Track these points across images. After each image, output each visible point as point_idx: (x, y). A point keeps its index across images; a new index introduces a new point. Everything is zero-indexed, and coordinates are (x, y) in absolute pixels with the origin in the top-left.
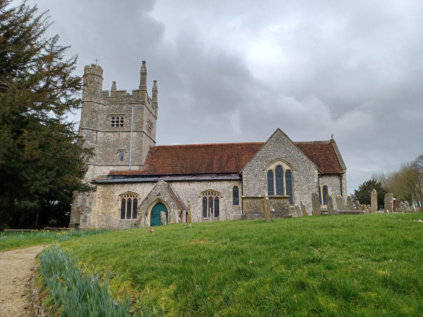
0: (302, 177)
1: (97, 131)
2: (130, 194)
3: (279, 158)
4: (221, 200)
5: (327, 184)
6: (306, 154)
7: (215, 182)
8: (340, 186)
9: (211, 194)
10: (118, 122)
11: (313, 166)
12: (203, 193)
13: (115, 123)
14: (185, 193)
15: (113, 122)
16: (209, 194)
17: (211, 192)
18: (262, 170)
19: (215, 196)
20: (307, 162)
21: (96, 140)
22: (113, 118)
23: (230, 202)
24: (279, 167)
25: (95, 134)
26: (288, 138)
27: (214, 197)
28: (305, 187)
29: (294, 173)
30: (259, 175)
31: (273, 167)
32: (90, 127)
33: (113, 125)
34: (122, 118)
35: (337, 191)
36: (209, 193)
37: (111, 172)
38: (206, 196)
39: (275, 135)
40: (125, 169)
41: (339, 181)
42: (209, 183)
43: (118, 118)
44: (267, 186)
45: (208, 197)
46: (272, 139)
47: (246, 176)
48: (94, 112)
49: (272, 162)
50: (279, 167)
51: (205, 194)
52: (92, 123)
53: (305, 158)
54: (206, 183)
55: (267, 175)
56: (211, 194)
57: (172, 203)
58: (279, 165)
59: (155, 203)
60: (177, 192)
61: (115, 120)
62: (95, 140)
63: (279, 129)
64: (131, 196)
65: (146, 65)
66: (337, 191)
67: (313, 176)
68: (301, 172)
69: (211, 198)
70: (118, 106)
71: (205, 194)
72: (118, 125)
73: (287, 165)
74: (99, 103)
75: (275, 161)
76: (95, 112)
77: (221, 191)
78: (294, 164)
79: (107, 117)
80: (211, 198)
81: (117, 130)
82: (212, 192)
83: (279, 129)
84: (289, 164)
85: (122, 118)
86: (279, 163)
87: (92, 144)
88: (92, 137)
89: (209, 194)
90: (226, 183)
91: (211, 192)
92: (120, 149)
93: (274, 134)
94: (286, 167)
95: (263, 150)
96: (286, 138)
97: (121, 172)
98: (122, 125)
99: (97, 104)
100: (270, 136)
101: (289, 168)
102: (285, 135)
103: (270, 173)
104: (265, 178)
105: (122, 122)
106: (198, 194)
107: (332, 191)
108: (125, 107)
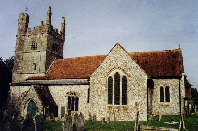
0: (134, 82)
1: (23, 52)
3: (117, 66)
4: (80, 99)
5: (169, 85)
6: (138, 62)
7: (76, 86)
8: (179, 86)
9: (73, 94)
10: (34, 46)
11: (143, 72)
12: (68, 93)
13: (33, 46)
14: (57, 93)
16: (72, 95)
17: (73, 93)
18: (104, 76)
19: (76, 96)
20: (138, 69)
21: (23, 58)
22: (32, 44)
23: (85, 100)
24: (117, 75)
25: (22, 54)
26: (125, 50)
27: (75, 96)
28: (136, 90)
29: (128, 78)
30: (101, 81)
31: (112, 74)
32: (19, 50)
34: (37, 43)
35: (176, 91)
36: (72, 94)
37: (29, 77)
38: (74, 96)
39: (115, 48)
40: (37, 75)
41: (179, 82)
42: (72, 86)
43: (35, 44)
44: (107, 89)
45: (71, 96)
46: (112, 52)
47: (92, 81)
48: (21, 41)
49: (111, 70)
50: (117, 75)
51: (69, 94)
52: (20, 48)
53: (137, 65)
54: (70, 86)
55: (108, 80)
56: (73, 94)
57: (38, 101)
58: (117, 72)
59: (29, 101)
60: (52, 92)
61: (33, 44)
62: (21, 58)
63: (117, 43)
65: (51, 8)
66: (176, 91)
67: (143, 80)
68: (133, 78)
69: (73, 97)
71: (69, 94)
72: (34, 48)
73: (123, 72)
74: (25, 36)
75: (113, 69)
76: (23, 41)
77: (79, 92)
78: (128, 71)
79: (29, 43)
80: (73, 97)
81: (33, 51)
82: (73, 93)
83: (117, 43)
84: (124, 71)
85: (37, 43)
86: (117, 70)
87: (19, 61)
88: (19, 57)
89: (72, 95)
90: (83, 86)
91: (73, 93)
92: (35, 63)
93: (113, 48)
94: (122, 74)
95: (105, 61)
96: (123, 51)
97: (32, 77)
98: (36, 48)
99: (23, 37)
100: (111, 49)
101: (125, 75)
102: (123, 48)
103: (110, 78)
104: (105, 83)
105: (37, 45)
106: (65, 94)
107: (173, 90)
108: (38, 36)
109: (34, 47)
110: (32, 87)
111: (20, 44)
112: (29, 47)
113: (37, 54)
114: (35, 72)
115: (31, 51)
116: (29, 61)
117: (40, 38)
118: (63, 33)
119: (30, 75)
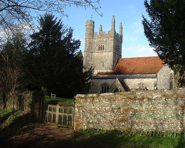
2: (105, 84)
10: (101, 47)
15: (99, 47)
22: (99, 46)
25: (91, 54)
33: (99, 49)
43: (101, 46)
52: (90, 49)
64: (106, 85)
70: (102, 39)
76: (91, 43)
105: (103, 47)
108: (104, 40)
109: (101, 48)
110: (117, 79)
111: (90, 46)
112: (97, 48)
113: (104, 54)
114: (104, 68)
115: (99, 51)
116: (97, 60)
117: (106, 41)
118: (122, 37)
119: (101, 71)
